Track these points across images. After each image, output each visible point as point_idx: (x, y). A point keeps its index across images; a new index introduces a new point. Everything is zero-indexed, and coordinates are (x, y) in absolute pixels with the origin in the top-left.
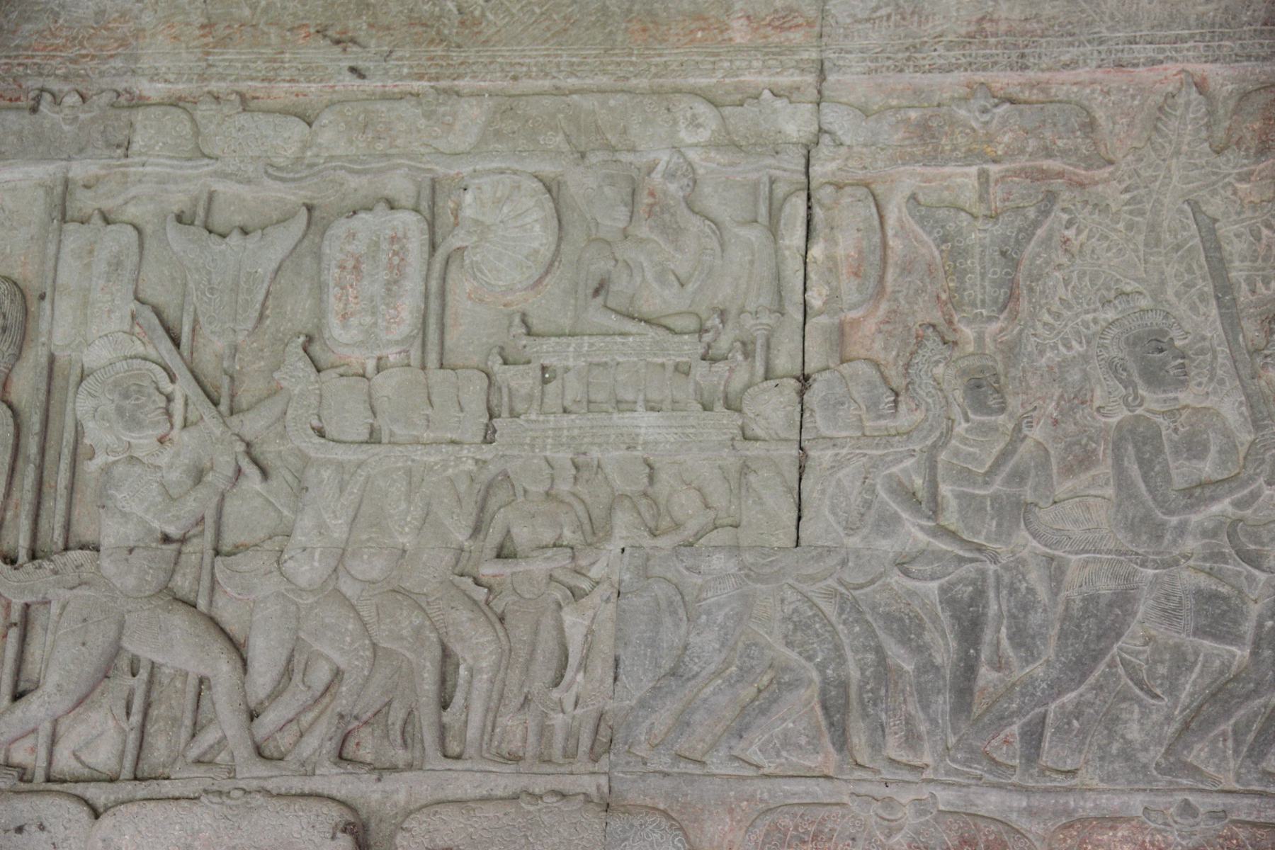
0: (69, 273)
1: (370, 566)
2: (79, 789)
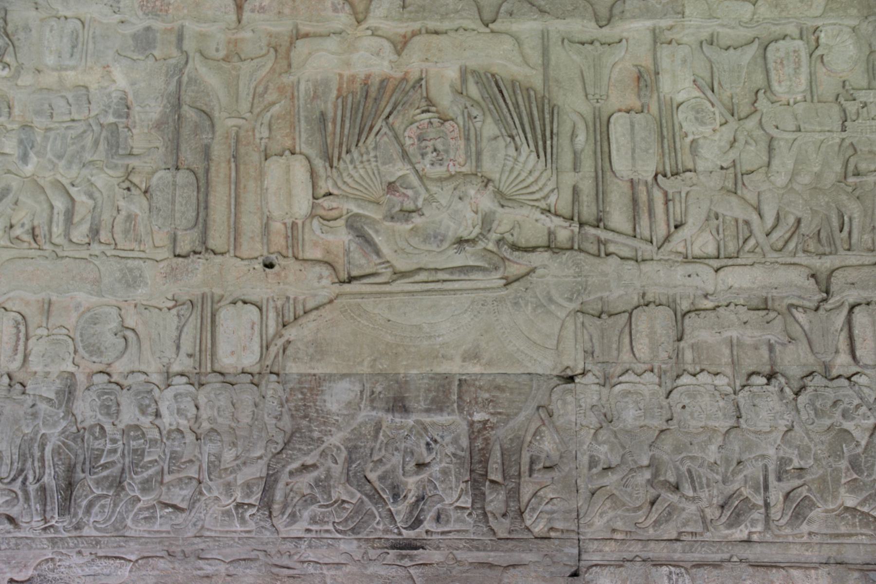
0: (665, 64)
2: (707, 261)
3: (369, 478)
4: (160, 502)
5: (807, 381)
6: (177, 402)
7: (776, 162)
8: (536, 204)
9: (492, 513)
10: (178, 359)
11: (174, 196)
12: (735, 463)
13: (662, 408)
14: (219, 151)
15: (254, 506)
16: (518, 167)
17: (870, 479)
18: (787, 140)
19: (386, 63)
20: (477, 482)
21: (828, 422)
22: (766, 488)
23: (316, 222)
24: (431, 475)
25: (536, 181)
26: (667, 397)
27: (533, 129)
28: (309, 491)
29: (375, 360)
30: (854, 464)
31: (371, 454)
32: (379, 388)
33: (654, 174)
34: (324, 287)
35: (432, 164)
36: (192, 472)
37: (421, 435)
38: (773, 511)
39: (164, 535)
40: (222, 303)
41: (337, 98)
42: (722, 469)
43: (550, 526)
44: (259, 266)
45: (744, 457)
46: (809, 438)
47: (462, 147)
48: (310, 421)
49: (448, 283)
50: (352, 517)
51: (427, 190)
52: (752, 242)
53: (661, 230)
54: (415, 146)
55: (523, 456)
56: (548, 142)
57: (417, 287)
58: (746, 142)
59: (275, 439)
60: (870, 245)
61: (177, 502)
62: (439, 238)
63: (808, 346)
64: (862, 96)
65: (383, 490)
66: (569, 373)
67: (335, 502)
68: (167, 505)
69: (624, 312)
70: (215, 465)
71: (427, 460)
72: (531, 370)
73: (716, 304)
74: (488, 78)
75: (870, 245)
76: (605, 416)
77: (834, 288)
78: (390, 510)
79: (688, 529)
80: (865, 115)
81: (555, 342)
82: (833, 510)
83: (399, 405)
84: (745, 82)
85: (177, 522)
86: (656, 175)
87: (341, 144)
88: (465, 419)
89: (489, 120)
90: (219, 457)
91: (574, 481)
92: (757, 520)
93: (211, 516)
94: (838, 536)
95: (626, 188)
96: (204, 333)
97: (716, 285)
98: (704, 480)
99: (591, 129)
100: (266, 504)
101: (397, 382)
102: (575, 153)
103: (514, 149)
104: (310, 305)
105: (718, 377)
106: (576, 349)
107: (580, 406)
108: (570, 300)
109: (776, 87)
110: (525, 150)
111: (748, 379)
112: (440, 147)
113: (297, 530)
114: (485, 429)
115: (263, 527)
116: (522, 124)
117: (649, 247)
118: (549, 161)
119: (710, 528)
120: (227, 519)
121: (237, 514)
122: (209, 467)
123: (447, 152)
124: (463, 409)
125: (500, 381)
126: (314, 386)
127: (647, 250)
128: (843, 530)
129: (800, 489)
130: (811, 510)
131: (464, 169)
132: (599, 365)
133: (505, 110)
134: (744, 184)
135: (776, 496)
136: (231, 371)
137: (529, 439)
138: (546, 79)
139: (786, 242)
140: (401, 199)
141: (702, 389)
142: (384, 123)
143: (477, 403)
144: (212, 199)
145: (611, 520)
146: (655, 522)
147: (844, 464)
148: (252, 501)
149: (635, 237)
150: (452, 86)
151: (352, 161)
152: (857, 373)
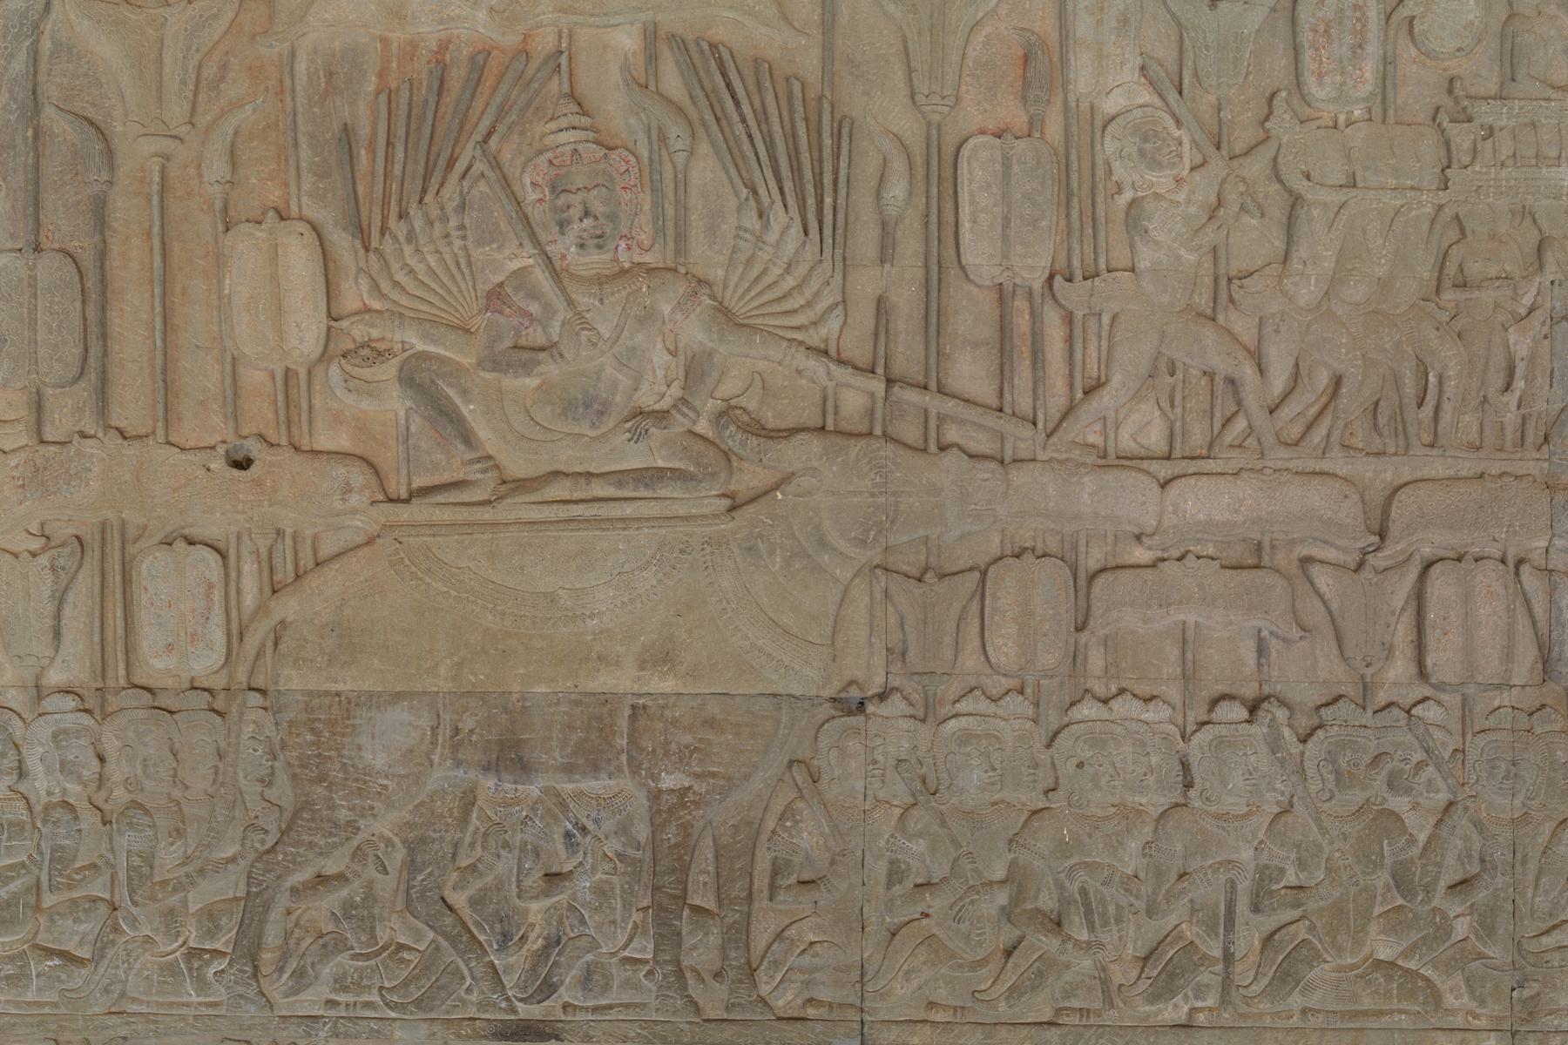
1: (1356, 291)
2: (1145, 464)
3: (450, 901)
4: (36, 946)
5: (1326, 713)
6: (58, 747)
7: (1301, 252)
8: (799, 336)
9: (694, 970)
10: (59, 659)
11: (33, 310)
12: (1173, 876)
13: (1036, 766)
14: (123, 207)
15: (224, 954)
16: (764, 256)
17: (1427, 908)
18: (1325, 205)
19: (482, 15)
20: (668, 909)
21: (1358, 797)
22: (1230, 924)
23: (334, 370)
24: (574, 897)
25: (800, 286)
26: (1049, 746)
27: (796, 169)
28: (331, 927)
29: (461, 664)
30: (1401, 881)
31: (454, 855)
32: (469, 723)
33: (1047, 272)
34: (354, 512)
35: (582, 246)
36: (98, 888)
37: (556, 819)
38: (1239, 968)
39: (46, 1010)
40: (140, 545)
41: (378, 93)
42: (1147, 889)
43: (807, 995)
44: (218, 464)
45: (1195, 864)
46: (1320, 828)
47: (647, 207)
48: (329, 788)
49: (612, 504)
50: (417, 978)
51: (570, 303)
52: (1240, 425)
53: (1057, 398)
54: (546, 206)
55: (759, 858)
56: (828, 200)
57: (547, 513)
58: (1243, 208)
59: (260, 822)
60: (1474, 436)
61: (70, 946)
62: (596, 406)
63: (1334, 643)
64: (1486, 113)
65: (478, 924)
66: (854, 693)
67: (384, 948)
68: (50, 953)
69: (971, 569)
70: (142, 873)
71: (567, 868)
72: (778, 688)
73: (1159, 554)
74: (702, 52)
75: (1474, 436)
76: (924, 782)
77: (1395, 529)
78: (493, 964)
79: (1075, 1003)
80: (1488, 154)
81: (828, 631)
82: (1353, 967)
83: (510, 757)
84: (1248, 73)
85: (70, 985)
86: (1051, 277)
87: (385, 202)
88: (642, 785)
89: (704, 148)
90: (149, 860)
91: (857, 911)
92: (1207, 986)
93: (137, 975)
94: (1356, 1014)
95: (987, 304)
96: (109, 606)
97: (1161, 515)
98: (1111, 909)
99: (920, 171)
100: (249, 951)
101: (506, 710)
102: (884, 224)
103: (755, 216)
104: (326, 550)
105: (1151, 705)
106: (871, 645)
107: (875, 762)
108: (862, 543)
109: (1310, 81)
110: (778, 217)
111: (1211, 710)
112: (598, 208)
113: (310, 1001)
114: (683, 805)
115: (241, 996)
116: (773, 159)
117: (1026, 431)
118: (828, 241)
119: (1117, 1001)
120: (170, 979)
121: (190, 969)
122: (129, 878)
123: (613, 217)
124: (639, 766)
125: (714, 709)
126: (335, 717)
127: (1022, 439)
128: (1367, 1003)
129: (1293, 926)
130: (1312, 967)
131: (648, 258)
132: (916, 678)
133: (739, 129)
134: (1231, 300)
135: (1248, 940)
136: (170, 683)
137: (771, 824)
138: (828, 50)
139: (1309, 427)
140: (515, 321)
141: (1119, 729)
142: (478, 153)
143: (666, 753)
144: (113, 316)
145: (926, 983)
146: (1012, 989)
147: (1382, 878)
148: (218, 946)
149: (1001, 410)
150: (626, 68)
151: (411, 237)
152: (1425, 699)
